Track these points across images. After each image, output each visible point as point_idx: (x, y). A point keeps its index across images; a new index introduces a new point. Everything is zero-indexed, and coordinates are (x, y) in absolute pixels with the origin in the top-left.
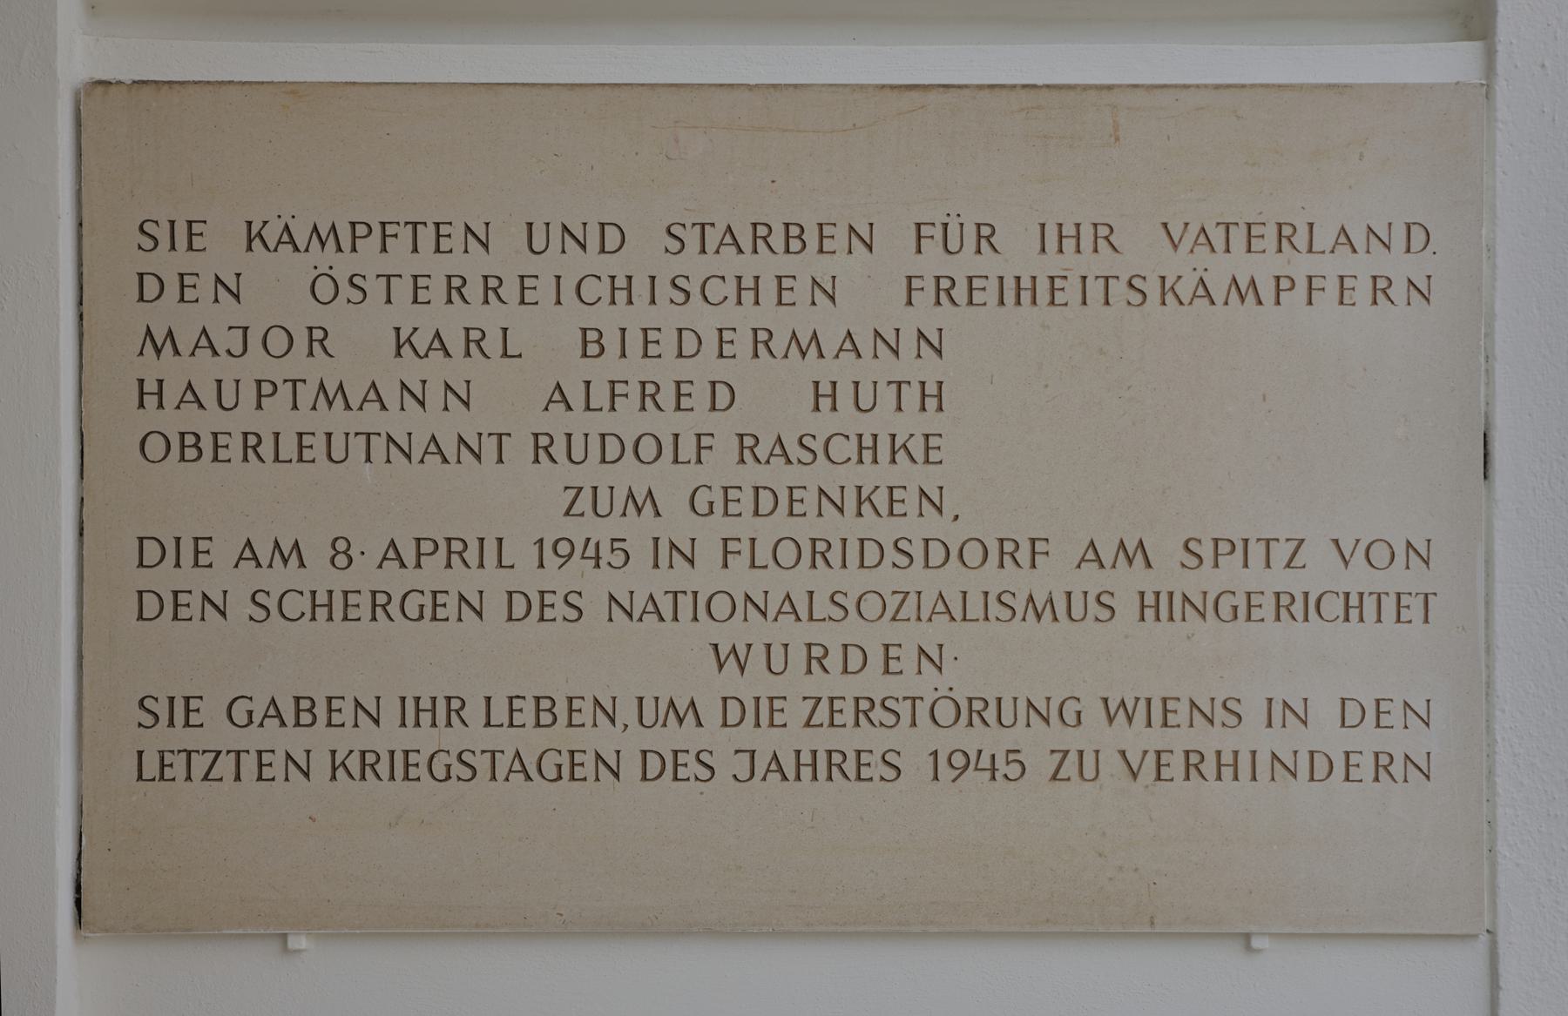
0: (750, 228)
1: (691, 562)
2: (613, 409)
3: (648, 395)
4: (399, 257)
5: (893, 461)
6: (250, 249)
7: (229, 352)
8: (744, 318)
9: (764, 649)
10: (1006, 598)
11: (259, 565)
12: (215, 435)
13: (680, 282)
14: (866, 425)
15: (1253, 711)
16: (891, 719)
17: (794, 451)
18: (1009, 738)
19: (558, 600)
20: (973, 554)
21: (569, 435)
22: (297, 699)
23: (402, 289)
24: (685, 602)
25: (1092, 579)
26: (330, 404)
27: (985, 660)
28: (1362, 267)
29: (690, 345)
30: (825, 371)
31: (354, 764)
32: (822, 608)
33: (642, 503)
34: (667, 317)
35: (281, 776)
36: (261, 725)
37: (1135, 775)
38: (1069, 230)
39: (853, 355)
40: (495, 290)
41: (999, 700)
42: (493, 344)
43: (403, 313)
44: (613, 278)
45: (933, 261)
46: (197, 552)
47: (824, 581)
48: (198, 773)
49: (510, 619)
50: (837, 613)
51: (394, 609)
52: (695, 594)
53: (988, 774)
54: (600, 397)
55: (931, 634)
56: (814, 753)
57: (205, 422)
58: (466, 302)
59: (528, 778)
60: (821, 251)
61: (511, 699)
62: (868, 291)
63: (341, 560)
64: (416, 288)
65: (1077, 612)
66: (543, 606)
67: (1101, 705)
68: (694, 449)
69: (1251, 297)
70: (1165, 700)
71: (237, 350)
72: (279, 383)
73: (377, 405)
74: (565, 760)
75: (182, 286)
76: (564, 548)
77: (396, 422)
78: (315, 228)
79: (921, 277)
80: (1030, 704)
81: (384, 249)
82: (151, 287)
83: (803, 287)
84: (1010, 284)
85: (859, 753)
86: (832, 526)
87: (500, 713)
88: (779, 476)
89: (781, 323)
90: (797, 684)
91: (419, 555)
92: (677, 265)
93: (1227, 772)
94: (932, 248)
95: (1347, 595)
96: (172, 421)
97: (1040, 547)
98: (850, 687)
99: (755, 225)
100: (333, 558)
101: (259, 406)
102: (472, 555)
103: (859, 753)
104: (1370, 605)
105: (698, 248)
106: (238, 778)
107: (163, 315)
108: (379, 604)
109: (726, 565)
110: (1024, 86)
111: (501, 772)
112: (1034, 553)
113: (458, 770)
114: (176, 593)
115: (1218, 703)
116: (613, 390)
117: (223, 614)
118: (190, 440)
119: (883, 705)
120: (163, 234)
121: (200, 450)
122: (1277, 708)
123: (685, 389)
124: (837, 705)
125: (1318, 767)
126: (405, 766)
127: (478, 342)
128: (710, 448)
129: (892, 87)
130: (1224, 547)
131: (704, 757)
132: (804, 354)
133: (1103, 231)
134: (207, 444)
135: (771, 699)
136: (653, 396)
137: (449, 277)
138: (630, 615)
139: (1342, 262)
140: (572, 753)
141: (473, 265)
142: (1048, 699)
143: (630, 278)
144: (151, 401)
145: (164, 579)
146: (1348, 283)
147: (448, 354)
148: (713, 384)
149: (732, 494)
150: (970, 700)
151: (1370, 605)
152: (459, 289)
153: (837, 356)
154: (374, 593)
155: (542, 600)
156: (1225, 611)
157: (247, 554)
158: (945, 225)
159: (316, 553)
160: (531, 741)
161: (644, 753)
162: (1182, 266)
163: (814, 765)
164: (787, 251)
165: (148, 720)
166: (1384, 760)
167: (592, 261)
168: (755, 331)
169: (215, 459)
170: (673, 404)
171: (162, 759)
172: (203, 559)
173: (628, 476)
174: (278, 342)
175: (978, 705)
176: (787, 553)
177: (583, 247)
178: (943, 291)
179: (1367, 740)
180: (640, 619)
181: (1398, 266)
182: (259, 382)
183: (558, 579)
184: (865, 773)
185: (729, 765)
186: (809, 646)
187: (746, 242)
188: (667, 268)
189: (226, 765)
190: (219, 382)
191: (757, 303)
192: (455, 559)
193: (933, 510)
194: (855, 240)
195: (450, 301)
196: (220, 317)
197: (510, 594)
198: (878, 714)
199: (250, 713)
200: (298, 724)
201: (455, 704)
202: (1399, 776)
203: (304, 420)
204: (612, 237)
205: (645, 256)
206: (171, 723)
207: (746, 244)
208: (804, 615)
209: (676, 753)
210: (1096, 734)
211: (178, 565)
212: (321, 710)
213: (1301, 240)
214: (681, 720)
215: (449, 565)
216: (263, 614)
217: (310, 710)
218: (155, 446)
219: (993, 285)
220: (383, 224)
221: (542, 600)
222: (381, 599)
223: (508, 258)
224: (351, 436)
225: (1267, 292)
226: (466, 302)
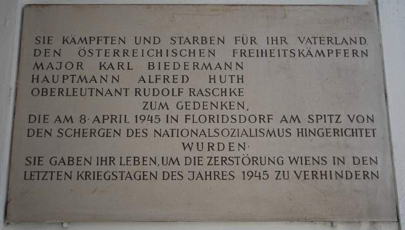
2: (156, 82)
3: (166, 79)
4: (102, 45)
5: (231, 95)
8: (190, 60)
14: (224, 86)
15: (330, 160)
16: (231, 163)
17: (204, 93)
18: (264, 168)
20: (252, 119)
23: (102, 53)
25: (285, 126)
27: (258, 147)
31: (84, 175)
34: (171, 59)
37: (299, 178)
42: (125, 66)
43: (102, 59)
45: (240, 46)
47: (212, 126)
52: (178, 130)
54: (153, 79)
56: (210, 172)
59: (132, 179)
62: (223, 54)
64: (106, 53)
70: (306, 157)
71: (59, 68)
76: (143, 118)
77: (98, 86)
80: (269, 159)
81: (98, 43)
82: (38, 53)
83: (206, 52)
86: (215, 112)
87: (124, 162)
88: (200, 99)
89: (201, 61)
90: (206, 153)
91: (104, 119)
94: (240, 43)
95: (353, 130)
96: (40, 86)
98: (220, 154)
101: (63, 82)
104: (359, 132)
107: (41, 59)
108: (92, 133)
110: (262, 5)
112: (269, 119)
113: (112, 177)
115: (320, 158)
118: (45, 90)
122: (336, 160)
125: (349, 176)
126: (97, 176)
132: (207, 69)
133: (283, 39)
134: (49, 92)
135: (198, 157)
138: (160, 135)
139: (344, 47)
140: (144, 172)
144: (35, 81)
150: (253, 157)
151: (359, 132)
158: (243, 38)
160: (132, 169)
162: (304, 47)
167: (152, 46)
170: (172, 81)
174: (69, 66)
175: (255, 159)
176: (203, 119)
179: (361, 168)
181: (359, 48)
183: (141, 126)
187: (191, 41)
189: (49, 175)
196: (54, 60)
198: (228, 161)
199: (56, 161)
200: (69, 164)
201: (112, 159)
203: (75, 85)
204: (157, 40)
205: (165, 45)
206: (34, 164)
212: (75, 161)
213: (334, 41)
216: (61, 135)
217: (72, 161)
218: (35, 92)
219: (255, 52)
220: (98, 37)
223: (130, 45)
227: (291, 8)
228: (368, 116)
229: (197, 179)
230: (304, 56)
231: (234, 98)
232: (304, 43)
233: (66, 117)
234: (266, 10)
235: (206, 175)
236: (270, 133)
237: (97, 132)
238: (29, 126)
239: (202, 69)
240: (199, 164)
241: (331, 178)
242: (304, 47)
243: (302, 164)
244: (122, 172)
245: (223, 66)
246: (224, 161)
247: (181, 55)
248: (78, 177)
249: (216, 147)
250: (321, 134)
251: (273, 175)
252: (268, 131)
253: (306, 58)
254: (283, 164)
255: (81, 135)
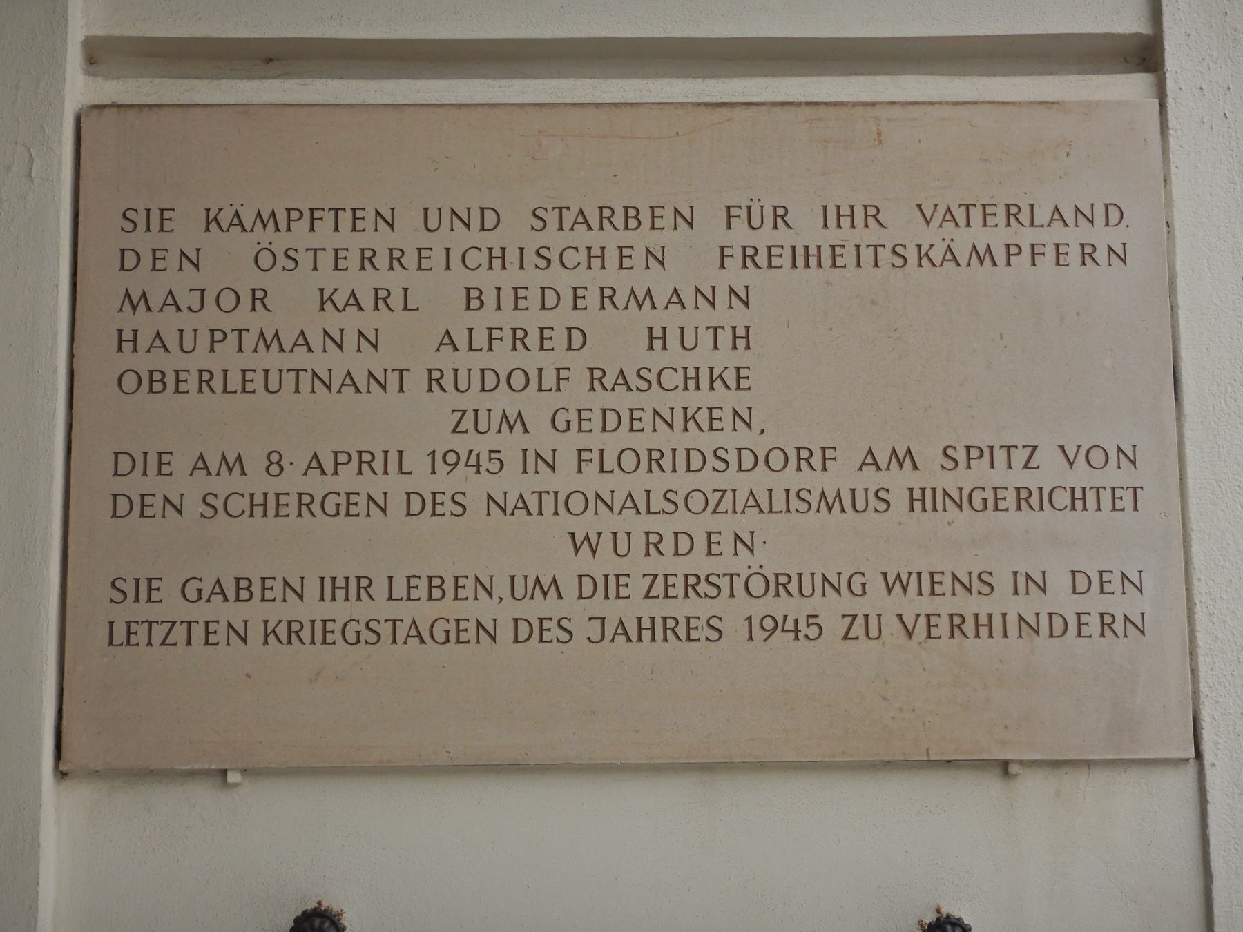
0: (597, 211)
1: (553, 468)
2: (490, 349)
3: (518, 339)
4: (324, 236)
5: (712, 388)
6: (208, 230)
7: (189, 308)
8: (593, 279)
9: (611, 536)
10: (803, 494)
11: (209, 473)
12: (177, 372)
13: (543, 252)
14: (691, 360)
15: (1003, 581)
16: (714, 592)
17: (634, 381)
18: (809, 606)
19: (447, 499)
20: (776, 460)
21: (456, 370)
22: (238, 580)
23: (326, 259)
24: (548, 500)
25: (871, 480)
26: (268, 347)
27: (787, 544)
28: (1073, 237)
29: (551, 299)
30: (657, 319)
31: (282, 631)
32: (658, 503)
33: (514, 422)
34: (533, 278)
35: (223, 641)
36: (208, 600)
37: (910, 634)
38: (845, 210)
39: (679, 306)
40: (398, 259)
41: (800, 575)
42: (396, 300)
43: (327, 277)
44: (490, 249)
45: (740, 235)
46: (160, 463)
47: (658, 482)
48: (157, 639)
49: (408, 514)
50: (670, 508)
51: (316, 507)
52: (556, 493)
53: (792, 635)
54: (480, 340)
55: (747, 522)
56: (653, 619)
57: (169, 362)
58: (375, 268)
59: (422, 641)
60: (653, 227)
61: (409, 578)
62: (690, 260)
63: (274, 469)
64: (337, 258)
65: (860, 505)
66: (434, 504)
67: (881, 578)
68: (555, 380)
69: (987, 260)
70: (932, 574)
71: (196, 307)
72: (228, 332)
73: (305, 348)
74: (452, 627)
75: (155, 258)
76: (451, 458)
77: (317, 361)
78: (259, 214)
79: (731, 247)
80: (825, 578)
81: (312, 229)
82: (130, 259)
83: (639, 256)
84: (800, 251)
85: (688, 618)
86: (664, 439)
87: (400, 590)
88: (622, 400)
89: (622, 282)
90: (638, 565)
91: (336, 464)
92: (542, 239)
93: (984, 631)
94: (739, 225)
95: (1073, 489)
96: (144, 362)
97: (829, 454)
98: (681, 566)
99: (601, 208)
100: (268, 468)
101: (212, 350)
102: (378, 465)
103: (688, 618)
104: (1091, 496)
105: (557, 226)
106: (189, 643)
107: (139, 280)
108: (304, 504)
109: (580, 471)
110: (808, 104)
111: (401, 637)
112: (824, 459)
113: (366, 635)
114: (143, 496)
115: (974, 576)
116: (490, 335)
117: (180, 512)
118: (157, 376)
119: (707, 580)
120: (141, 220)
121: (165, 384)
122: (1021, 580)
123: (547, 333)
124: (671, 580)
125: (1056, 626)
126: (323, 633)
127: (384, 299)
128: (567, 379)
129: (707, 105)
130: (974, 453)
131: (564, 623)
132: (640, 306)
133: (872, 211)
134: (170, 379)
135: (617, 576)
136: (522, 340)
137: (362, 250)
138: (504, 511)
139: (1058, 233)
140: (458, 621)
141: (382, 241)
142: (839, 574)
143: (503, 249)
144: (127, 347)
145: (135, 485)
146: (1062, 249)
147: (361, 309)
148: (569, 329)
149: (585, 415)
150: (777, 575)
151: (1091, 496)
152: (370, 259)
153: (666, 308)
154: (300, 495)
155: (434, 499)
156: (977, 503)
157: (200, 465)
158: (749, 208)
159: (255, 464)
160: (425, 612)
161: (516, 620)
162: (934, 237)
163: (653, 629)
164: (627, 228)
165: (118, 597)
166: (1108, 620)
167: (473, 236)
168: (602, 288)
169: (177, 391)
170: (538, 346)
171: (129, 628)
172: (165, 469)
173: (503, 401)
174: (228, 300)
175: (783, 580)
176: (629, 461)
177: (468, 226)
178: (749, 257)
179: (1094, 603)
180: (512, 514)
181: (1101, 237)
182: (212, 331)
183: (446, 482)
184: (693, 635)
185: (584, 629)
186: (647, 533)
187: (594, 221)
188: (534, 241)
189: (179, 633)
190: (181, 331)
191: (603, 267)
192: (365, 467)
193: (744, 426)
194: (679, 219)
195: (363, 268)
196: (183, 282)
197: (408, 494)
198: (703, 587)
199: (200, 591)
200: (238, 599)
201: (364, 583)
202: (1120, 632)
203: (247, 360)
204: (490, 219)
205: (515, 233)
206: (137, 600)
207: (594, 222)
208: (643, 508)
209: (541, 620)
210: (877, 601)
211: (145, 474)
212: (257, 589)
213: (1025, 217)
214: (545, 594)
215: (360, 472)
216: (212, 512)
217: (248, 589)
218: (130, 382)
219: (787, 252)
220: (312, 210)
221: (434, 499)
222: (306, 499)
223: (408, 235)
224: (284, 373)
225: (1000, 256)
226: (375, 268)
227: (896, 112)
228: (1119, 449)
229: (613, 640)
230: (934, 265)
231: (723, 398)
232: (935, 222)
233: (224, 458)
234: (820, 119)
235: (640, 629)
236: (828, 503)
237: (318, 501)
238: (113, 485)
239: (626, 308)
240: (618, 597)
241: (1005, 636)
242: (934, 237)
243: (920, 594)
244: (394, 621)
245: (688, 298)
246: (693, 586)
247: (563, 264)
248: (266, 636)
249: (667, 546)
250: (977, 503)
251: (834, 626)
252: (823, 495)
253: (938, 269)
254: (864, 592)
255: (271, 511)
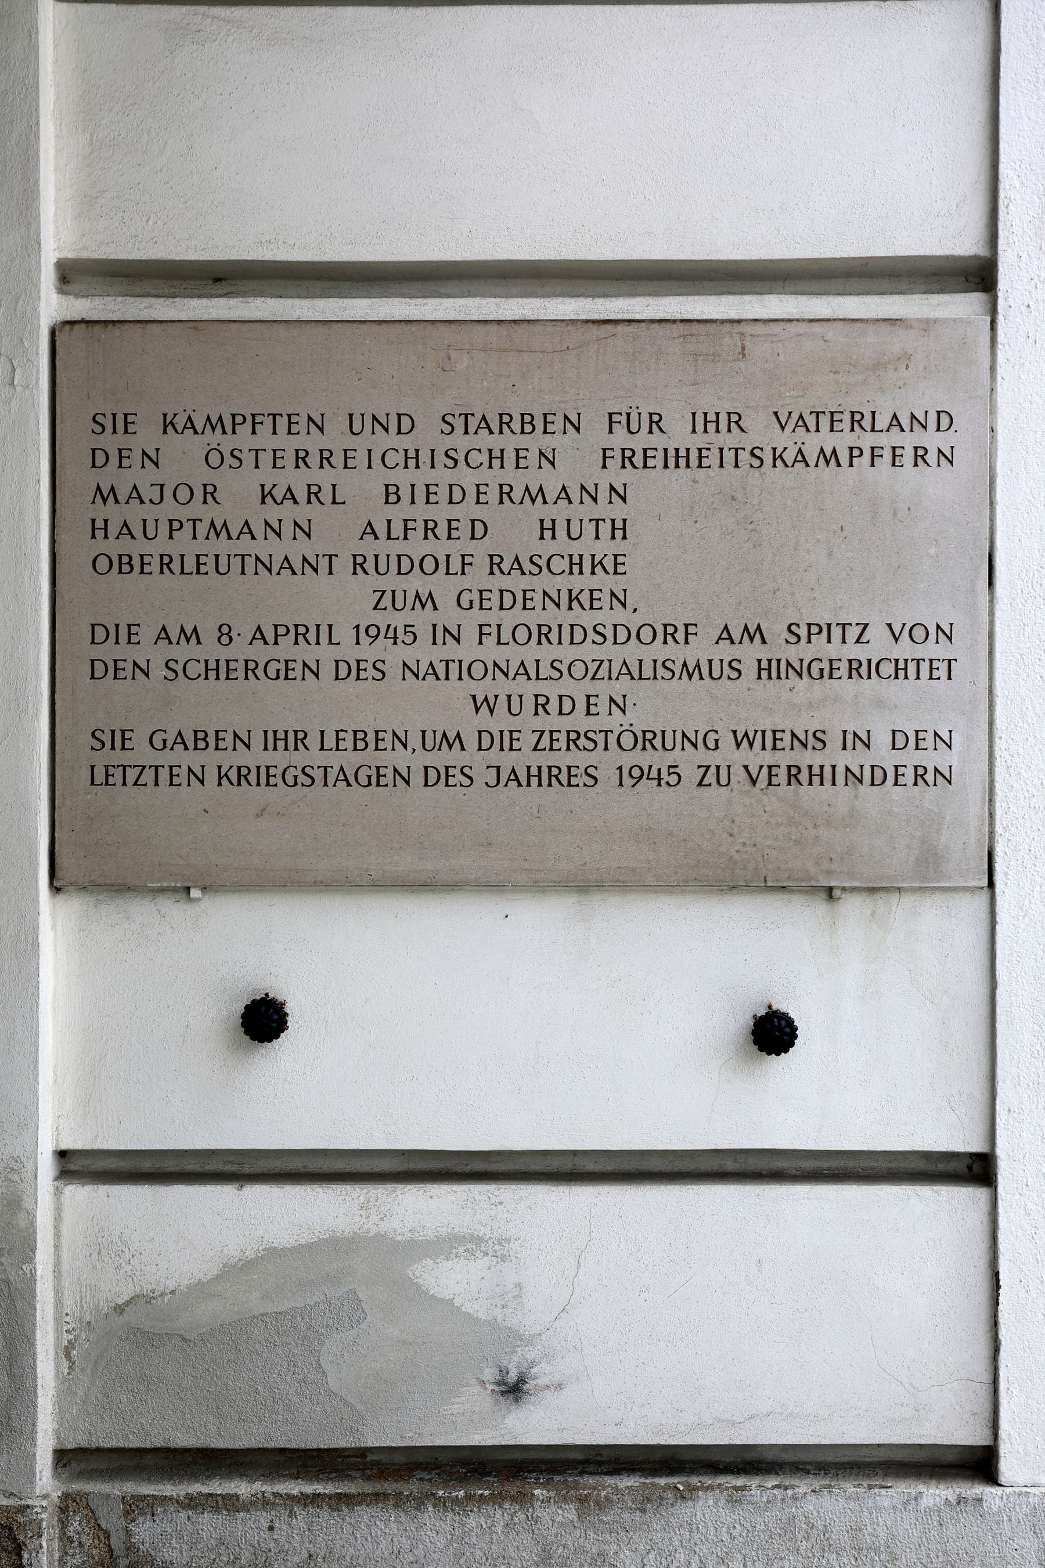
2: (406, 538)
3: (430, 529)
4: (264, 438)
5: (593, 573)
6: (165, 432)
7: (151, 501)
8: (493, 477)
9: (506, 698)
10: (668, 664)
11: (170, 643)
12: (142, 556)
14: (576, 548)
15: (834, 740)
16: (591, 745)
17: (527, 566)
18: (670, 758)
19: (369, 666)
20: (646, 634)
23: (266, 458)
24: (454, 667)
25: (726, 651)
27: (653, 706)
28: (908, 441)
29: (457, 495)
31: (233, 775)
32: (545, 671)
33: (425, 601)
34: (442, 476)
36: (172, 749)
37: (754, 782)
38: (711, 417)
40: (327, 459)
41: (663, 732)
42: (326, 496)
43: (267, 475)
45: (620, 439)
47: (547, 653)
48: (130, 780)
52: (460, 662)
53: (655, 782)
54: (397, 530)
55: (620, 687)
56: (540, 768)
57: (137, 547)
59: (349, 785)
60: (545, 432)
61: (337, 732)
62: (577, 460)
63: (225, 639)
64: (275, 458)
66: (359, 670)
67: (731, 735)
69: (833, 461)
70: (774, 732)
71: (157, 500)
74: (373, 772)
75: (121, 458)
76: (373, 631)
77: (261, 548)
79: (613, 449)
80: (684, 735)
81: (254, 432)
82: (100, 459)
84: (671, 453)
85: (569, 767)
86: (552, 616)
87: (330, 742)
88: (516, 583)
89: (518, 480)
90: (529, 723)
91: (276, 636)
92: (449, 442)
93: (816, 780)
95: (897, 661)
96: (114, 547)
100: (219, 638)
101: (171, 537)
102: (312, 636)
103: (569, 767)
106: (157, 784)
108: (250, 669)
109: (481, 643)
110: (682, 321)
111: (331, 781)
112: (687, 634)
113: (302, 778)
114: (116, 661)
115: (810, 734)
117: (147, 675)
118: (125, 559)
120: (108, 423)
122: (850, 737)
123: (454, 524)
125: (878, 777)
126: (266, 777)
127: (316, 494)
128: (471, 564)
129: (594, 322)
130: (814, 630)
131: (466, 770)
134: (136, 562)
135: (511, 732)
136: (433, 530)
139: (895, 438)
140: (378, 768)
141: (313, 443)
142: (697, 731)
144: (99, 534)
145: (108, 652)
146: (898, 452)
148: (473, 521)
149: (485, 595)
150: (644, 732)
153: (556, 503)
154: (246, 661)
156: (815, 672)
157: (163, 635)
158: (628, 414)
159: (209, 635)
160: (351, 760)
161: (426, 768)
162: (786, 441)
163: (539, 776)
164: (523, 432)
166: (921, 771)
167: (392, 440)
169: (142, 572)
172: (134, 639)
173: (416, 583)
174: (183, 494)
175: (649, 736)
176: (522, 634)
177: (387, 430)
178: (627, 459)
179: (910, 758)
180: (424, 679)
181: (932, 440)
182: (171, 521)
183: (369, 652)
186: (536, 696)
189: (149, 776)
191: (502, 467)
192: (300, 638)
193: (620, 605)
194: (568, 425)
196: (145, 478)
197: (337, 662)
199: (165, 741)
200: (196, 748)
201: (301, 735)
202: (931, 782)
203: (200, 546)
205: (427, 436)
206: (113, 748)
207: (496, 428)
208: (533, 675)
209: (447, 768)
210: (728, 754)
211: (117, 642)
212: (211, 740)
213: (867, 423)
215: (296, 643)
217: (204, 739)
218: (103, 564)
219: (660, 454)
220: (253, 416)
222: (251, 665)
223: (336, 438)
224: (232, 557)
227: (759, 329)
228: (938, 627)
229: (506, 785)
230: (787, 466)
231: (603, 581)
232: (789, 428)
233: (182, 629)
234: (692, 335)
235: (529, 776)
236: (689, 671)
237: (261, 666)
238: (89, 651)
239: (521, 503)
240: (511, 749)
241: (834, 784)
242: (784, 440)
243: (764, 748)
244: (326, 768)
245: (575, 495)
246: (574, 741)
247: (468, 464)
248: (220, 778)
249: (553, 706)
250: (815, 672)
251: (690, 774)
252: (685, 665)
253: (789, 469)
254: (717, 747)
255: (223, 675)
